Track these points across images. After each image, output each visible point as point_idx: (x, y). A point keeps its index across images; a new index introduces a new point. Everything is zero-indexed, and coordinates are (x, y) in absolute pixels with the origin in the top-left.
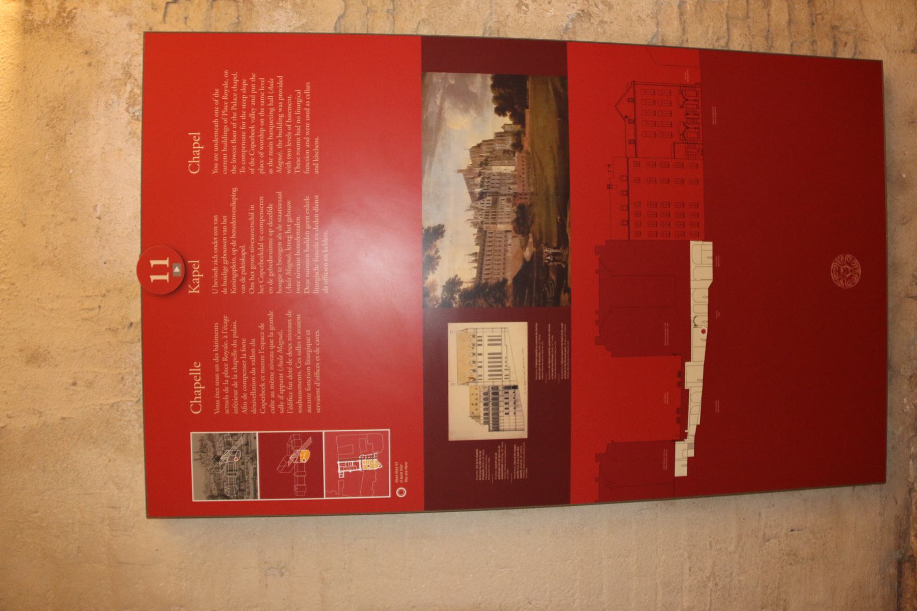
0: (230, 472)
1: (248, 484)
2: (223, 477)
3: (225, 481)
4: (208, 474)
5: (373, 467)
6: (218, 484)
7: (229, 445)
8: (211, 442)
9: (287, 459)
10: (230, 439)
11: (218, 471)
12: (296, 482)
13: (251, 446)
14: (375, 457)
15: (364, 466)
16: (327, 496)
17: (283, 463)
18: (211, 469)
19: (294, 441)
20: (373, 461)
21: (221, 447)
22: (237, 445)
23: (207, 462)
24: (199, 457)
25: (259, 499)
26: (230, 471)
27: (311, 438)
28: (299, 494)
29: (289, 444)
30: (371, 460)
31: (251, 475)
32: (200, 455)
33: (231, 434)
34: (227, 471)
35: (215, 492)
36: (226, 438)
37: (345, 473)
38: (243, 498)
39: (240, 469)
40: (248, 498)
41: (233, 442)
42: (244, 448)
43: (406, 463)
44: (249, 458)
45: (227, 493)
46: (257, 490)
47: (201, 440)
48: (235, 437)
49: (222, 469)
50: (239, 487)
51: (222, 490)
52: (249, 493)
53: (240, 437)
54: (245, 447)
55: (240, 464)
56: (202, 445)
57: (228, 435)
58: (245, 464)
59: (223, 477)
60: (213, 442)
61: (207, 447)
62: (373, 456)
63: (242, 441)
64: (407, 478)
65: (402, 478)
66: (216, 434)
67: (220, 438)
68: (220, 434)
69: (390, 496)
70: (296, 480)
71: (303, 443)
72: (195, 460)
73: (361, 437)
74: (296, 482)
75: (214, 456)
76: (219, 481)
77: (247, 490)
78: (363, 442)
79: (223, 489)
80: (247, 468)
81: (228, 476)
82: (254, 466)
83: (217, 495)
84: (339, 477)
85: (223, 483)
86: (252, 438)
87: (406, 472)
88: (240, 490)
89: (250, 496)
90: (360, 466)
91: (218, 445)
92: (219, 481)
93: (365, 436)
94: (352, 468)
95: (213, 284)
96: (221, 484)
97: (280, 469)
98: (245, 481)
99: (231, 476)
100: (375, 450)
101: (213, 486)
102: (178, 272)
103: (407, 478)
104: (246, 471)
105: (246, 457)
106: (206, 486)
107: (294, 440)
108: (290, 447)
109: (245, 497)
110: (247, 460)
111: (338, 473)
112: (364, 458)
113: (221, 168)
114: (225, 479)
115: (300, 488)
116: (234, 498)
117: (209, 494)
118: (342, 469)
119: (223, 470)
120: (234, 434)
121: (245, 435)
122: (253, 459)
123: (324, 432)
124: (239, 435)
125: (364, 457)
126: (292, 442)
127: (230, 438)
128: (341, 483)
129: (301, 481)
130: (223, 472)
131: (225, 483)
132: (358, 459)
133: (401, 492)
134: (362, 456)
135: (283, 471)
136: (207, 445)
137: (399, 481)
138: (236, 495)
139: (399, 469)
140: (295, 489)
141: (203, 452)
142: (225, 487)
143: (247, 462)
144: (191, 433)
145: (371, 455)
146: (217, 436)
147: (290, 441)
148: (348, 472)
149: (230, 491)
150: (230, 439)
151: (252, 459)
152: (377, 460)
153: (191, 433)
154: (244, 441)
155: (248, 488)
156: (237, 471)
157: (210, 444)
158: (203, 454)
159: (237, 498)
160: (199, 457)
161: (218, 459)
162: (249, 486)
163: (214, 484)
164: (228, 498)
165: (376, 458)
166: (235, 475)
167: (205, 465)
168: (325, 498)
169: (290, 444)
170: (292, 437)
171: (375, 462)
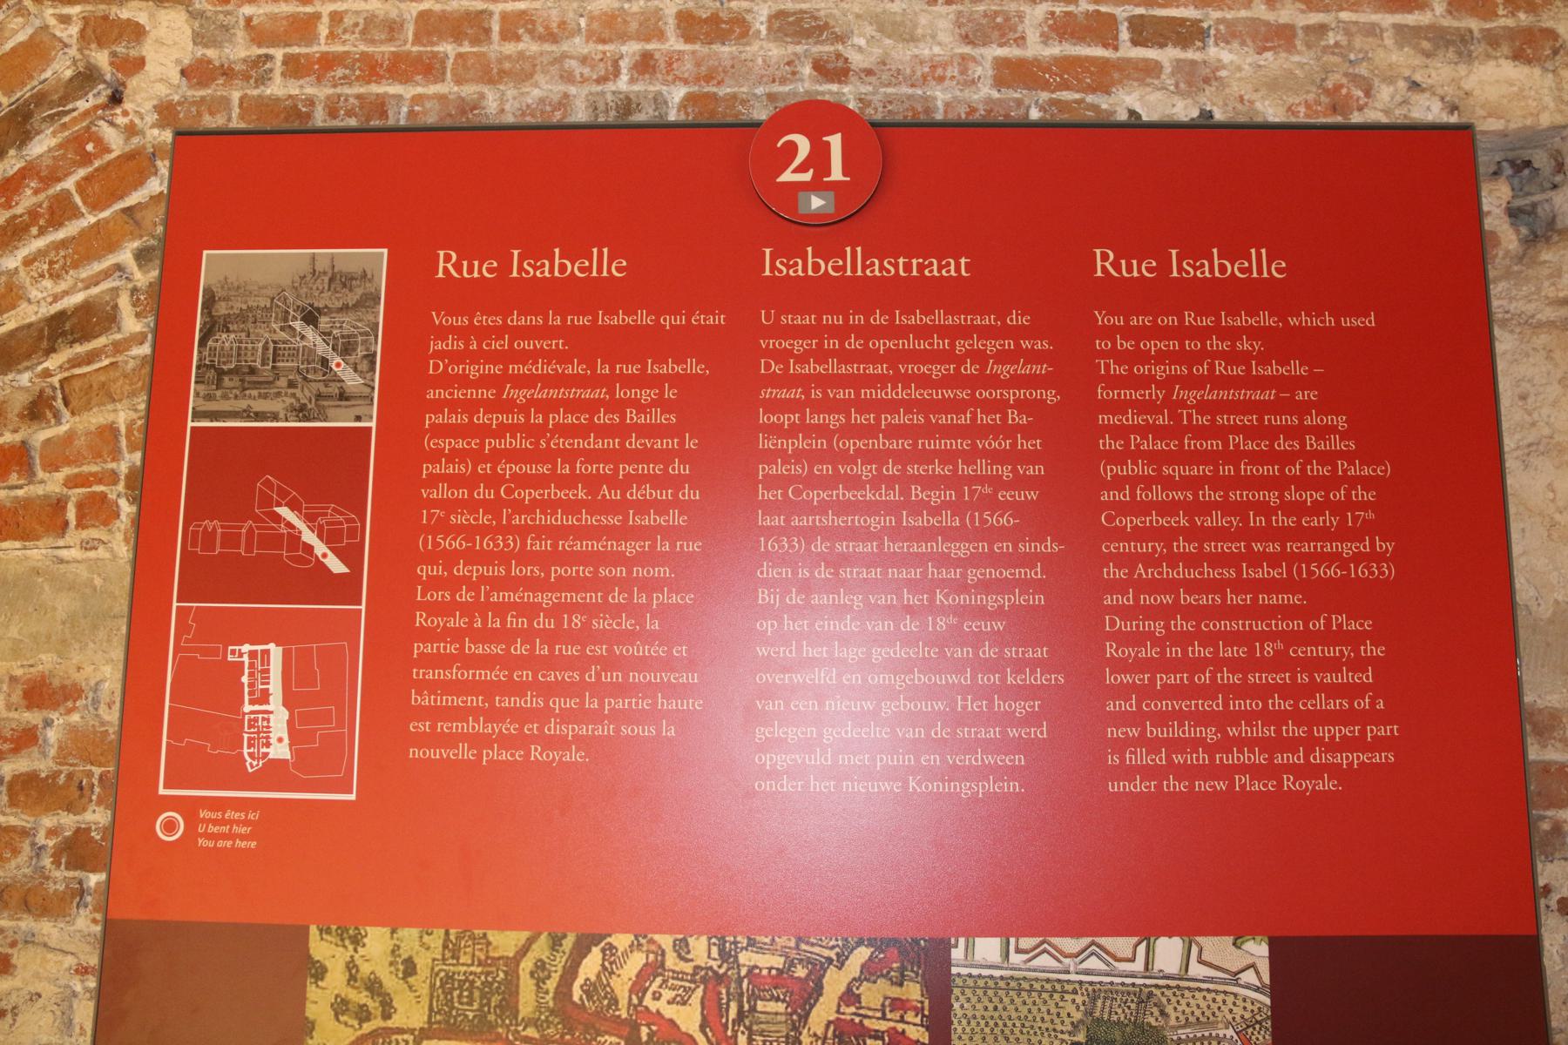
0: (271, 351)
1: (236, 397)
2: (262, 331)
3: (248, 336)
4: (270, 292)
5: (249, 746)
6: (242, 317)
7: (346, 349)
8: (358, 302)
9: (294, 506)
10: (361, 352)
11: (276, 318)
15: (256, 720)
19: (341, 523)
23: (304, 290)
24: (319, 268)
25: (190, 424)
26: (275, 349)
28: (195, 533)
29: (334, 510)
31: (260, 405)
32: (325, 273)
33: (375, 353)
34: (275, 342)
35: (221, 309)
36: (364, 342)
38: (196, 382)
39: (277, 377)
40: (197, 394)
41: (352, 358)
42: (334, 389)
43: (253, 844)
45: (217, 341)
46: (217, 421)
47: (364, 275)
48: (364, 366)
49: (282, 329)
50: (230, 372)
52: (209, 398)
54: (337, 391)
55: (290, 377)
56: (352, 279)
58: (291, 391)
59: (262, 331)
60: (357, 306)
63: (352, 380)
64: (211, 844)
65: (213, 829)
66: (376, 315)
67: (368, 326)
68: (378, 323)
69: (162, 791)
72: (313, 257)
73: (340, 710)
75: (318, 310)
76: (251, 320)
77: (219, 393)
78: (325, 718)
79: (228, 331)
80: (278, 394)
81: (261, 345)
82: (282, 415)
83: (214, 314)
84: (230, 648)
85: (242, 331)
87: (229, 844)
89: (201, 401)
90: (257, 707)
92: (251, 320)
93: (340, 724)
94: (251, 685)
96: (242, 326)
97: (268, 484)
98: (244, 389)
99: (260, 350)
100: (297, 753)
101: (238, 305)
103: (211, 844)
104: (272, 391)
105: (308, 394)
106: (238, 288)
108: (326, 514)
109: (201, 387)
111: (242, 645)
115: (209, 537)
116: (200, 360)
117: (219, 293)
118: (253, 654)
119: (278, 330)
120: (373, 363)
121: (369, 390)
122: (301, 411)
123: (363, 607)
124: (370, 374)
126: (341, 518)
128: (215, 652)
129: (231, 540)
130: (272, 331)
131: (243, 335)
133: (170, 826)
135: (260, 488)
136: (351, 290)
137: (204, 821)
139: (238, 822)
140: (209, 524)
141: (331, 280)
142: (232, 336)
143: (294, 395)
144: (385, 251)
147: (341, 514)
149: (222, 348)
150: (361, 352)
151: (303, 408)
153: (385, 251)
154: (355, 390)
155: (225, 397)
156: (273, 367)
157: (352, 299)
158: (326, 279)
159: (198, 367)
160: (319, 268)
161: (310, 318)
162: (229, 399)
163: (244, 307)
164: (203, 342)
167: (296, 285)
168: (175, 604)
169: (332, 514)
170: (353, 521)
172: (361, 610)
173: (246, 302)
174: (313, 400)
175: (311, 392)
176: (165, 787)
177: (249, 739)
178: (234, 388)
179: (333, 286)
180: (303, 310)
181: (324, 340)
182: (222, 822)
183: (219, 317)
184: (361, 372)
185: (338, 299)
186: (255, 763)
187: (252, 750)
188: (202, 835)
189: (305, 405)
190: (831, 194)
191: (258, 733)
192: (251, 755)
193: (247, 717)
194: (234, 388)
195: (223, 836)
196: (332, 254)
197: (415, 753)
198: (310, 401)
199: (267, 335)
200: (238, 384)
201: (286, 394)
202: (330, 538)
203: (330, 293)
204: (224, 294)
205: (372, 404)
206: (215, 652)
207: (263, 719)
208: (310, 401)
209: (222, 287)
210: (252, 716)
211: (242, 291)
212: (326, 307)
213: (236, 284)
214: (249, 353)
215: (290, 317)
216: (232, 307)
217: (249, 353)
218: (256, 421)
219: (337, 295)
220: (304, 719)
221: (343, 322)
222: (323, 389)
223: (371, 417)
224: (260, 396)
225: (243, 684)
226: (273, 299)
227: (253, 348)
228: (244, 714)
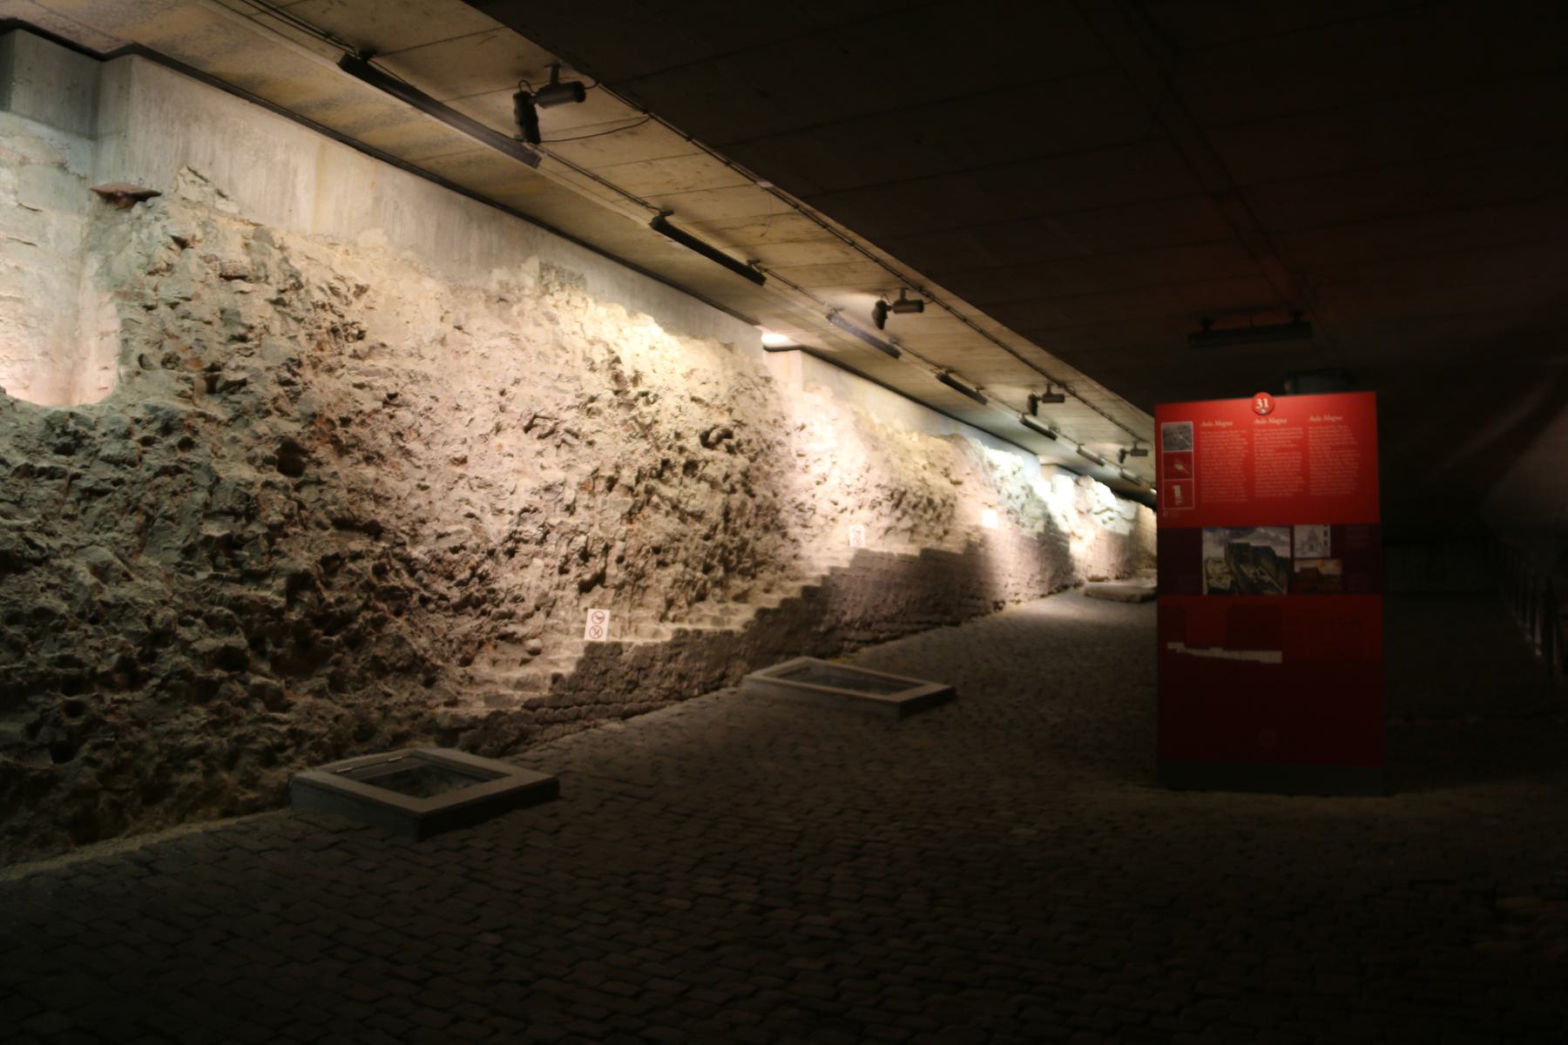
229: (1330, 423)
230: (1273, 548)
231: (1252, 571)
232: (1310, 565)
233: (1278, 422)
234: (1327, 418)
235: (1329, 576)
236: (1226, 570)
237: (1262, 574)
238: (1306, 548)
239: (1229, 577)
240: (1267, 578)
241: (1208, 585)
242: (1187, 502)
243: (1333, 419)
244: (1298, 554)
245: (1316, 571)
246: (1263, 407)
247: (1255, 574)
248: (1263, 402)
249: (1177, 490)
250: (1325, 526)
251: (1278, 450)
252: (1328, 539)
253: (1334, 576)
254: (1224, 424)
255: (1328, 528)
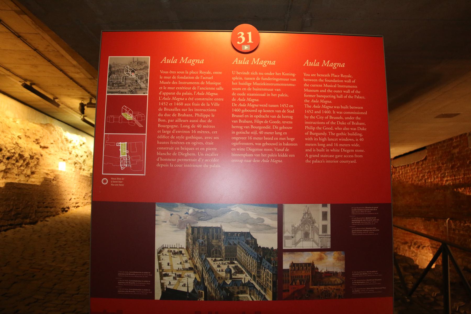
0: (124, 78)
1: (117, 89)
2: (122, 74)
3: (119, 75)
4: (124, 66)
5: (122, 165)
6: (118, 71)
7: (141, 78)
8: (144, 68)
10: (144, 79)
11: (125, 71)
12: (116, 117)
13: (140, 91)
14: (128, 165)
16: (105, 134)
17: (128, 110)
18: (127, 67)
19: (141, 116)
20: (126, 164)
21: (140, 73)
22: (140, 83)
23: (131, 65)
24: (135, 60)
25: (107, 94)
26: (125, 78)
27: (143, 126)
30: (126, 163)
32: (136, 62)
33: (148, 79)
34: (125, 76)
35: (113, 69)
36: (145, 77)
37: (120, 146)
38: (108, 85)
39: (126, 84)
40: (108, 88)
41: (142, 80)
42: (139, 87)
44: (132, 89)
45: (112, 76)
46: (113, 94)
47: (145, 62)
48: (145, 82)
49: (127, 74)
51: (114, 73)
52: (111, 89)
53: (145, 85)
54: (139, 87)
55: (129, 84)
57: (147, 78)
58: (129, 87)
59: (122, 74)
60: (143, 69)
61: (141, 65)
62: (129, 164)
63: (143, 85)
65: (114, 182)
67: (146, 73)
68: (148, 73)
70: (117, 117)
71: (140, 122)
72: (133, 57)
74: (116, 117)
75: (135, 69)
76: (120, 72)
77: (113, 88)
78: (138, 158)
79: (115, 74)
80: (126, 88)
81: (122, 77)
82: (127, 93)
83: (111, 70)
85: (118, 74)
86: (144, 92)
88: (113, 84)
89: (109, 89)
91: (141, 71)
93: (141, 159)
94: (122, 151)
95: (238, 72)
96: (118, 73)
97: (124, 107)
98: (118, 87)
100: (132, 166)
101: (117, 68)
102: (244, 48)
103: (114, 185)
104: (125, 87)
106: (117, 65)
107: (142, 117)
109: (109, 86)
110: (131, 87)
112: (127, 159)
113: (307, 78)
114: (120, 75)
115: (112, 119)
116: (108, 80)
117: (112, 66)
120: (147, 81)
121: (146, 87)
122: (131, 92)
123: (146, 134)
124: (147, 84)
125: (129, 159)
127: (145, 79)
128: (113, 144)
129: (116, 120)
131: (118, 75)
132: (127, 154)
133: (105, 181)
134: (129, 157)
135: (123, 108)
136: (142, 65)
138: (110, 81)
139: (120, 180)
140: (112, 116)
141: (138, 63)
142: (116, 75)
143: (130, 88)
144: (150, 57)
145: (130, 163)
146: (146, 71)
148: (120, 149)
149: (113, 78)
151: (132, 91)
152: (126, 166)
153: (150, 57)
154: (143, 87)
155: (114, 88)
156: (125, 82)
157: (142, 67)
158: (136, 63)
159: (108, 82)
160: (135, 60)
161: (133, 71)
162: (115, 89)
164: (109, 76)
165: (128, 166)
166: (123, 81)
168: (105, 134)
169: (139, 114)
171: (125, 165)
172: (145, 135)
173: (119, 68)
174: (134, 89)
175: (133, 87)
176: (103, 173)
177: (122, 163)
178: (116, 87)
179: (138, 64)
180: (131, 69)
181: (136, 76)
182: (116, 180)
183: (113, 71)
184: (145, 83)
185: (139, 67)
186: (123, 168)
187: (122, 165)
188: (112, 183)
189: (132, 90)
190: (249, 46)
191: (123, 161)
192: (122, 166)
193: (121, 158)
194: (116, 87)
195: (117, 183)
196: (138, 57)
197: (158, 165)
198: (133, 89)
199: (123, 75)
200: (117, 86)
201: (128, 88)
202: (139, 119)
203: (137, 66)
204: (114, 66)
205: (147, 90)
206: (113, 144)
207: (125, 158)
208: (133, 89)
209: (113, 64)
210: (122, 158)
211: (118, 65)
212: (136, 69)
213: (116, 64)
214: (120, 79)
215: (128, 71)
216: (115, 69)
217: (120, 79)
218: (121, 94)
219: (139, 66)
220: (134, 158)
221: (140, 72)
222: (136, 87)
223: (147, 93)
224: (122, 88)
225: (120, 151)
226: (124, 68)
227: (120, 78)
228: (120, 157)
229: (329, 70)
230: (254, 235)
231: (225, 267)
232: (304, 259)
233: (264, 63)
234: (326, 64)
235: (329, 274)
236: (187, 266)
237: (239, 271)
238: (299, 235)
239: (192, 274)
240: (245, 278)
241: (162, 285)
242: (137, 167)
243: (334, 65)
244: (287, 245)
245: (311, 266)
246: (246, 43)
247: (228, 271)
248: (246, 36)
249: (123, 147)
250: (324, 205)
251: (263, 100)
252: (328, 223)
253: (335, 274)
254: (192, 62)
255: (328, 209)
